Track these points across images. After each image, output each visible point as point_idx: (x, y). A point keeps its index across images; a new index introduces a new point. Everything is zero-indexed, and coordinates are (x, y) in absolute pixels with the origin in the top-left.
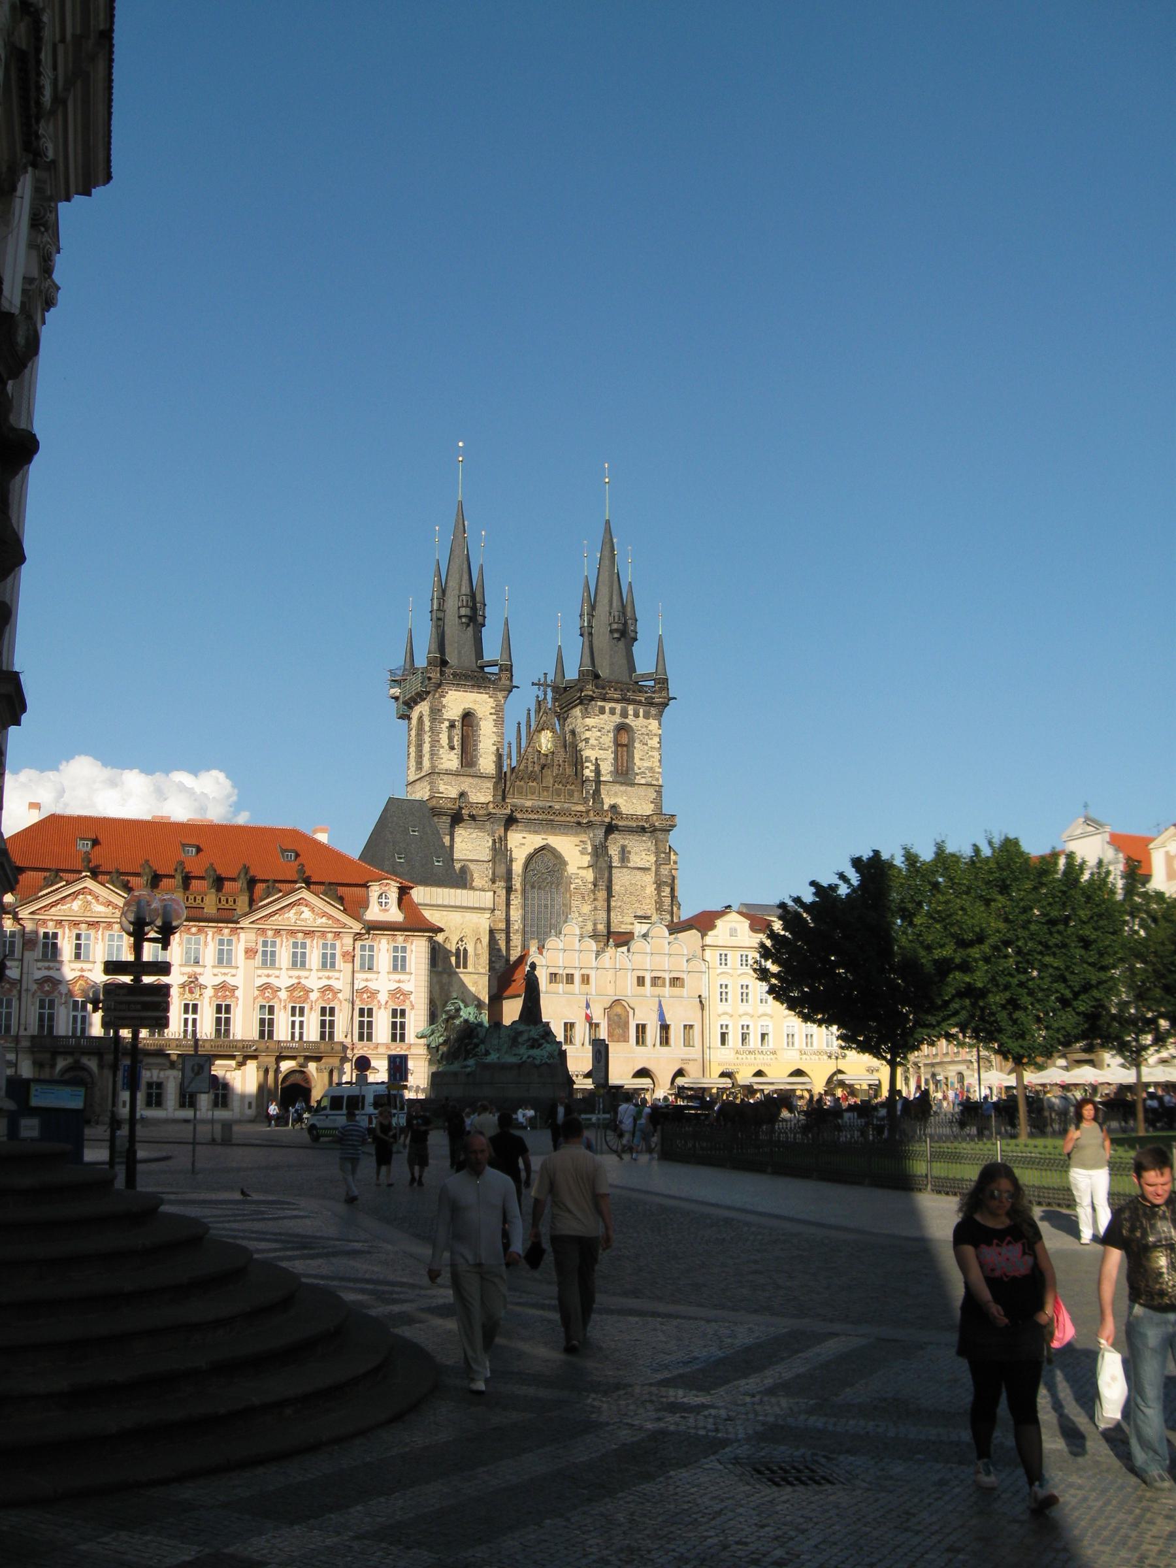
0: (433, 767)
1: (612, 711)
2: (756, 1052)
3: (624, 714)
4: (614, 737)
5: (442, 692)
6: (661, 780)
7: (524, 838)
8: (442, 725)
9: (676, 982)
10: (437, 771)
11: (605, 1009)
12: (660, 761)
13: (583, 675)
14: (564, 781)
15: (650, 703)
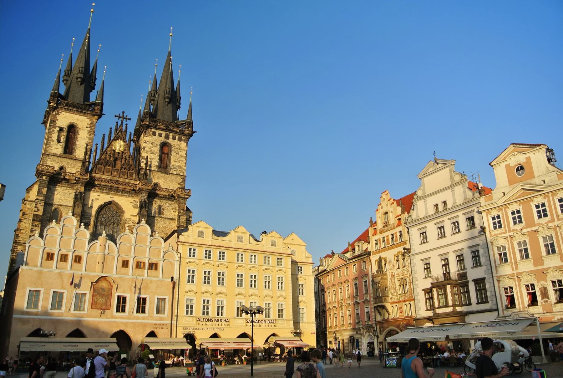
0: (46, 151)
1: (160, 135)
2: (214, 320)
3: (167, 137)
4: (160, 147)
5: (57, 112)
6: (185, 173)
7: (98, 196)
8: (55, 129)
9: (153, 266)
10: (47, 153)
11: (92, 283)
12: (185, 163)
13: (145, 114)
14: (127, 168)
15: (182, 133)
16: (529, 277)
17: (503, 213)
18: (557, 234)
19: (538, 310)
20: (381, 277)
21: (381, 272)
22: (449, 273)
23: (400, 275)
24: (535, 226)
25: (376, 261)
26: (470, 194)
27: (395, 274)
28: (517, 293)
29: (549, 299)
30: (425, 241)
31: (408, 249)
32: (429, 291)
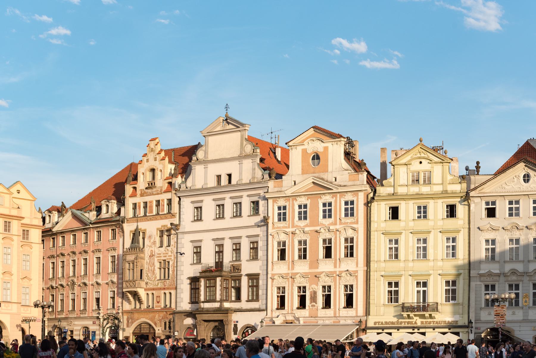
16: (303, 279)
17: (289, 205)
18: (336, 238)
19: (304, 313)
20: (136, 255)
21: (138, 249)
22: (222, 262)
23: (162, 255)
24: (318, 225)
25: (131, 231)
26: (259, 173)
27: (156, 254)
28: (288, 294)
29: (316, 304)
30: (199, 219)
31: (176, 226)
32: (194, 281)
